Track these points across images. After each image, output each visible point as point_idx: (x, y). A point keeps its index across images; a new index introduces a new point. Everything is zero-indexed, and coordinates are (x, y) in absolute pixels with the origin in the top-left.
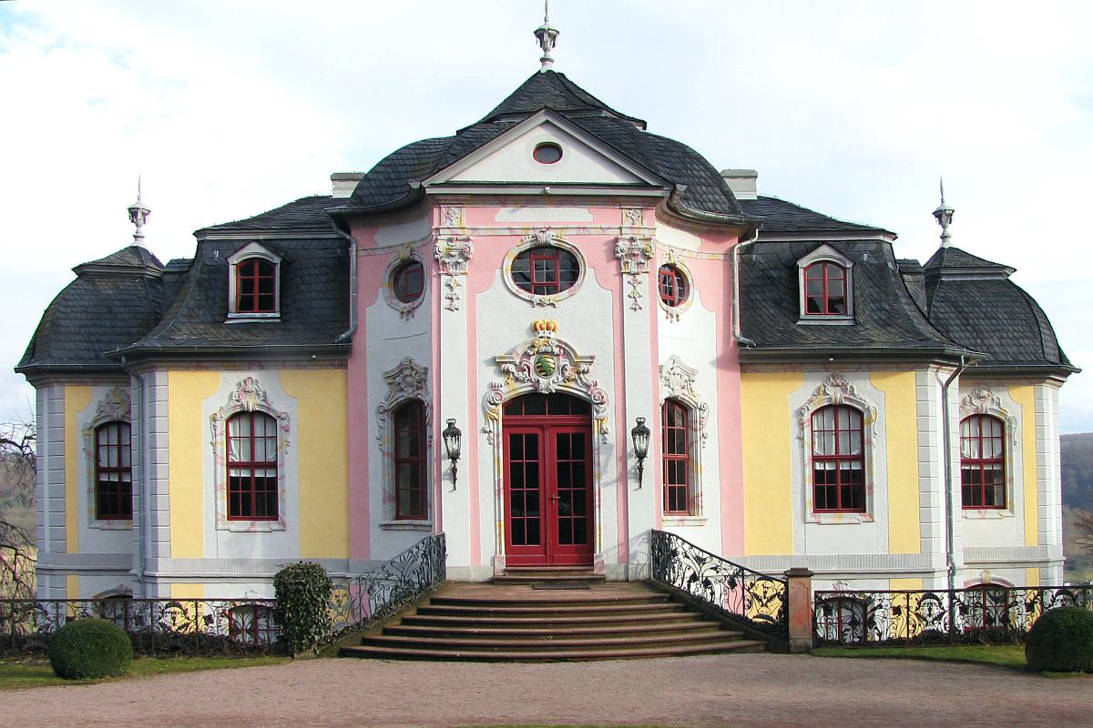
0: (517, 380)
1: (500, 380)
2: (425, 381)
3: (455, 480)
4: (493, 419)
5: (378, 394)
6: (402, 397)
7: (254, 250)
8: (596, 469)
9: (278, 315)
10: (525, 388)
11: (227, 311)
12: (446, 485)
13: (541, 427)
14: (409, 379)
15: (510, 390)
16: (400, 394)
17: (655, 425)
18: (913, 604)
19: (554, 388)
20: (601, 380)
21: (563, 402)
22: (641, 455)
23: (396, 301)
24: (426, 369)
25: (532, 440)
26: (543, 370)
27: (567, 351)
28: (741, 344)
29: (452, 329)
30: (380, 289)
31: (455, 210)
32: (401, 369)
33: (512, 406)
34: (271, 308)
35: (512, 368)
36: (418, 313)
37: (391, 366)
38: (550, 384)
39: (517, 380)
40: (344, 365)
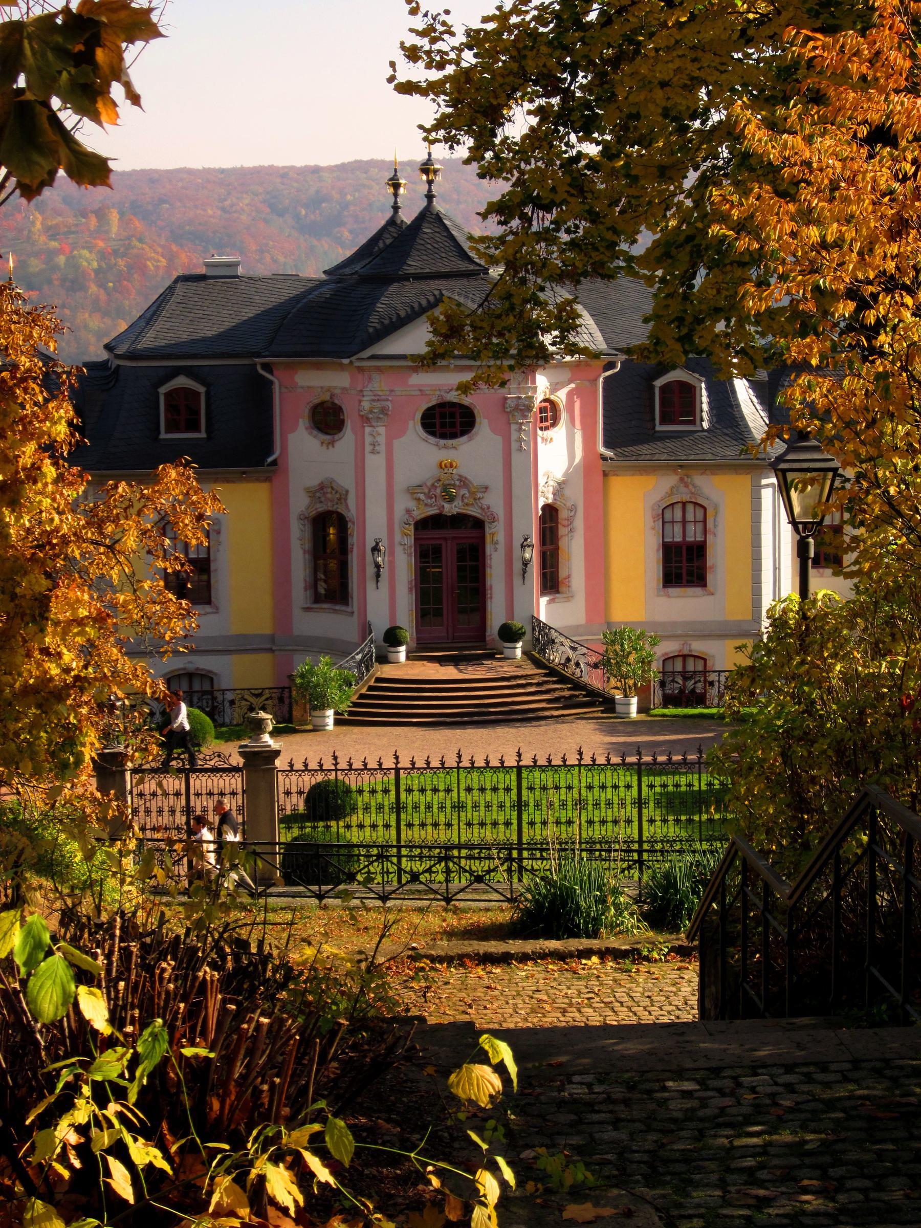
0: (426, 505)
1: (412, 504)
2: (346, 500)
3: (377, 581)
4: (407, 535)
5: (299, 503)
6: (321, 508)
7: (181, 381)
8: (488, 571)
9: (203, 435)
10: (433, 511)
11: (159, 433)
12: (370, 585)
13: (445, 539)
14: (329, 496)
15: (420, 513)
16: (318, 505)
17: (535, 539)
18: (723, 679)
19: (455, 511)
20: (494, 501)
21: (460, 520)
22: (526, 563)
23: (315, 432)
24: (347, 492)
25: (437, 551)
26: (451, 499)
27: (464, 482)
28: (604, 458)
29: (375, 465)
30: (301, 421)
31: (376, 376)
32: (322, 487)
33: (423, 525)
34: (197, 429)
35: (422, 496)
36: (337, 444)
37: (314, 482)
38: (450, 509)
39: (426, 505)
40: (268, 479)
